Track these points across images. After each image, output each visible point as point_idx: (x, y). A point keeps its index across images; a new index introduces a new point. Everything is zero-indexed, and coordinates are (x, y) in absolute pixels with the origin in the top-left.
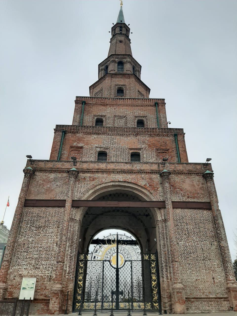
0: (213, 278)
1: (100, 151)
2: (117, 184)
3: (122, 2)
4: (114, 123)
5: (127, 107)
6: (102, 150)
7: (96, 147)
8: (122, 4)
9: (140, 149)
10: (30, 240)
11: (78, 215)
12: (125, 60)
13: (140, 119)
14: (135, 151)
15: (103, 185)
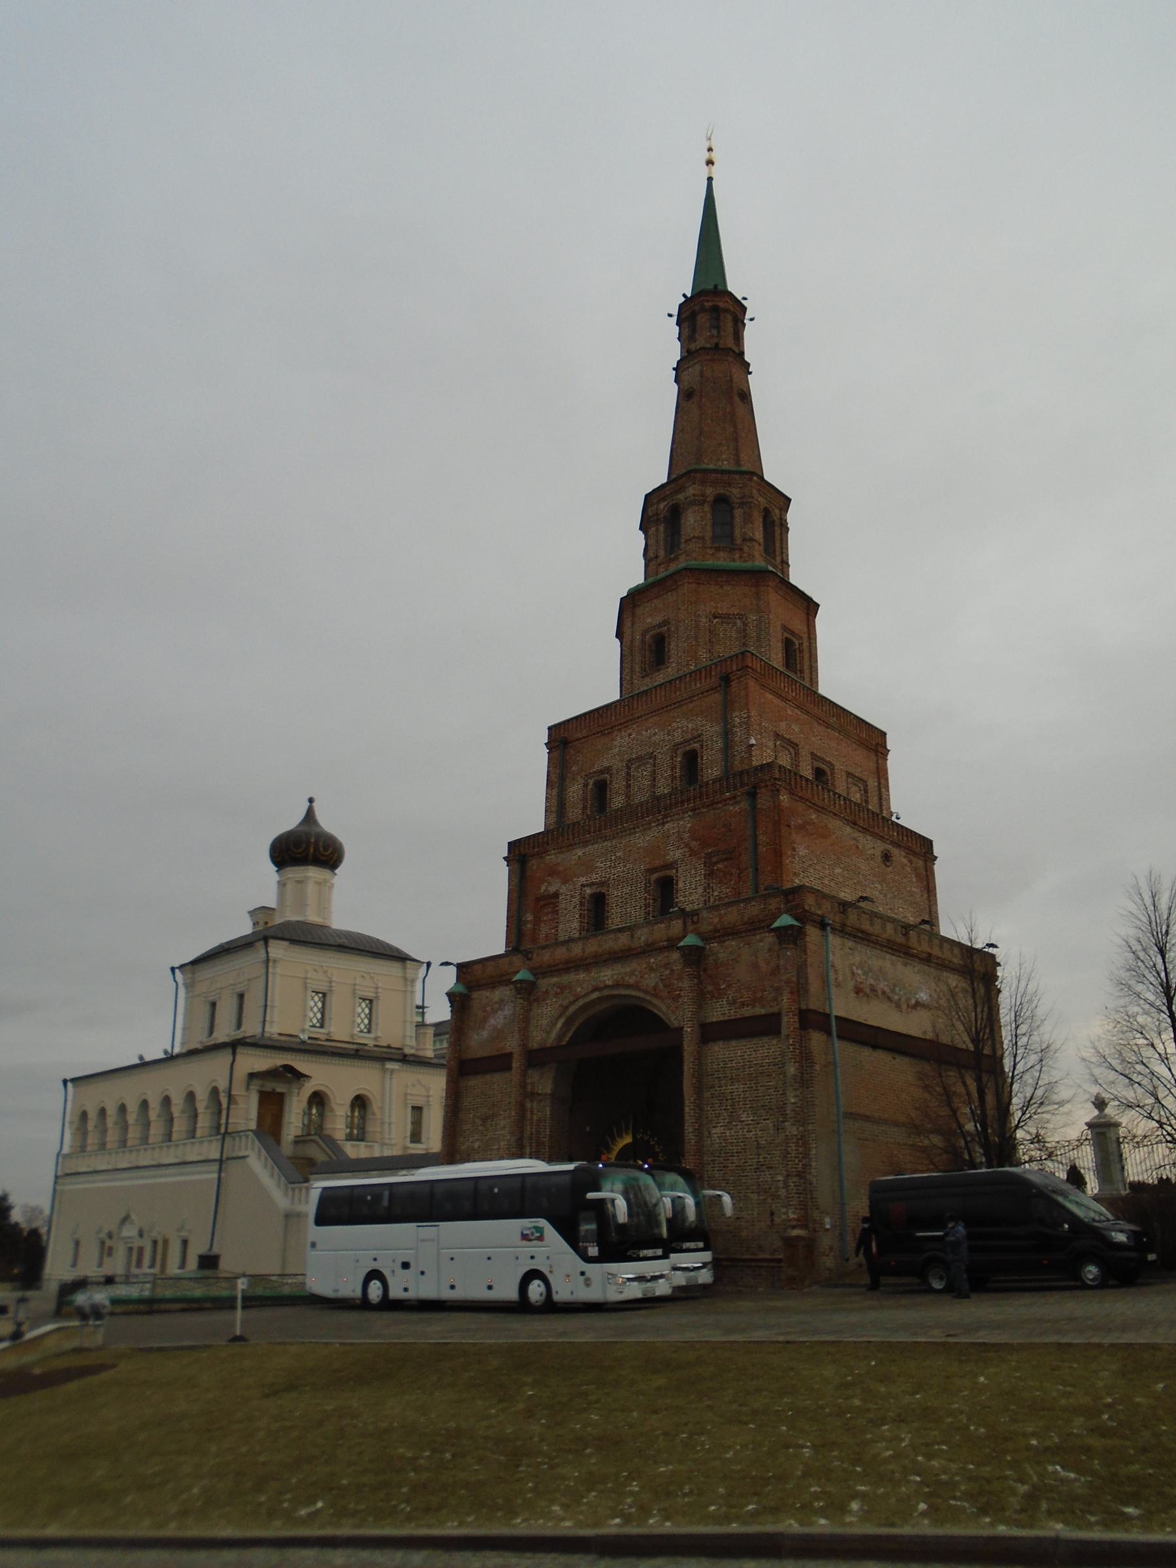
0: (772, 1214)
1: (592, 895)
2: (606, 992)
3: (710, 150)
4: (628, 786)
5: (656, 718)
6: (594, 890)
7: (583, 886)
8: (710, 162)
9: (671, 865)
10: (476, 1145)
11: (544, 1083)
12: (681, 496)
13: (687, 748)
14: (662, 874)
15: (581, 1002)
